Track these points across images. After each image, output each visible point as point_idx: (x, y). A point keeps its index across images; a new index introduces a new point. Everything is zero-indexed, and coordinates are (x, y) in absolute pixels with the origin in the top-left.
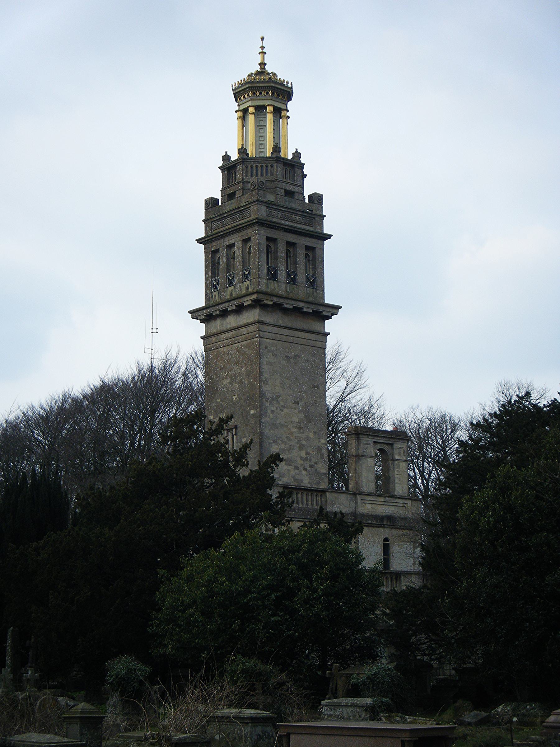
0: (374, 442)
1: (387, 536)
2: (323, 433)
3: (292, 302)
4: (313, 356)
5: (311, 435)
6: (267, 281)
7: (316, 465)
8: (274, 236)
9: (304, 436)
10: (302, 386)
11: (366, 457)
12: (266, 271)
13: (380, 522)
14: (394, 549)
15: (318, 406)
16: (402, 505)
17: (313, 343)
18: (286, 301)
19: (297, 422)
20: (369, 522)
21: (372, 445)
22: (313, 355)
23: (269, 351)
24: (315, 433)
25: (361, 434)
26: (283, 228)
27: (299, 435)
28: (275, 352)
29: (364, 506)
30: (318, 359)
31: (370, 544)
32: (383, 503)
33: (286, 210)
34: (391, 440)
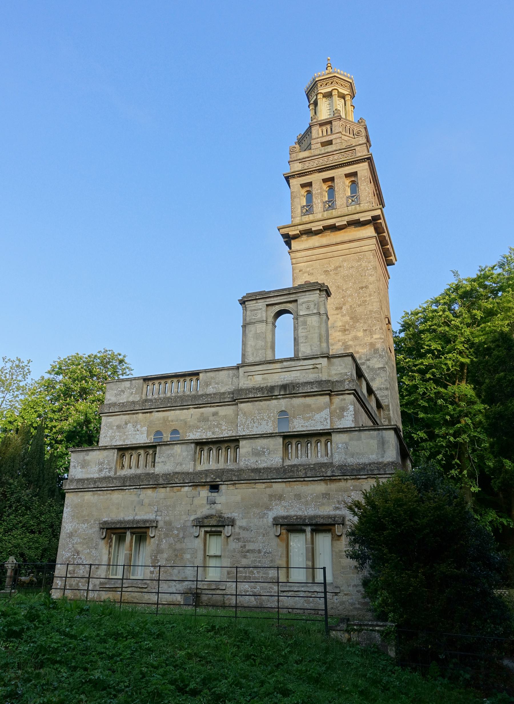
0: (268, 305)
1: (283, 409)
2: (375, 328)
3: (321, 223)
4: (358, 261)
5: (360, 334)
7: (368, 362)
9: (350, 337)
10: (345, 292)
11: (254, 323)
12: (299, 210)
13: (268, 393)
14: (295, 423)
15: (368, 304)
16: (311, 367)
17: (358, 250)
19: (340, 326)
20: (250, 396)
21: (264, 308)
22: (359, 260)
23: (305, 273)
24: (365, 331)
25: (247, 301)
27: (343, 338)
28: (311, 272)
29: (251, 379)
30: (366, 262)
31: (254, 422)
32: (280, 370)
34: (291, 296)
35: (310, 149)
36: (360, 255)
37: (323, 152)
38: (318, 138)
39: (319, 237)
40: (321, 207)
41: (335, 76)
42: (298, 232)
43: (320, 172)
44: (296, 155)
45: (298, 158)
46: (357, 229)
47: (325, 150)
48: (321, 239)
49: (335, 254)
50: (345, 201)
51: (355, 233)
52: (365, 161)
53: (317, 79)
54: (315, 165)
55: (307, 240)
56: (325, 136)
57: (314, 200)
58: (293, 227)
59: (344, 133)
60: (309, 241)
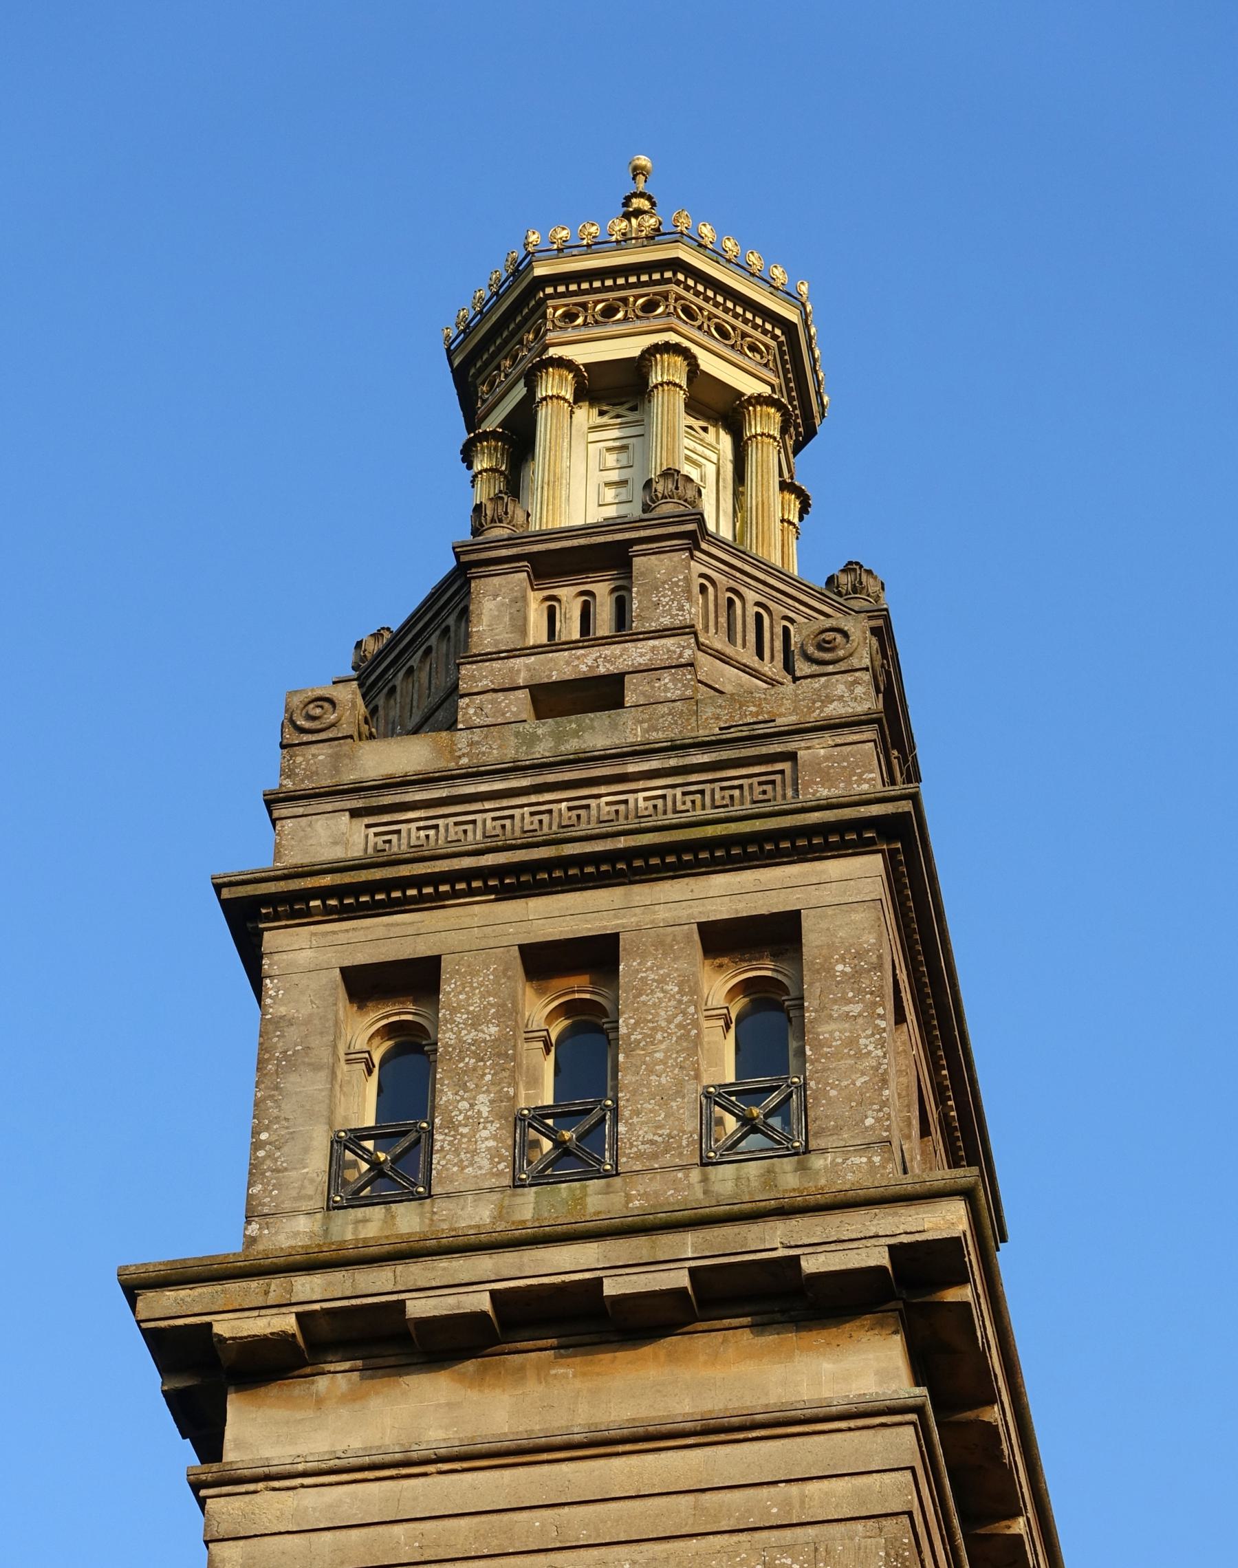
3: (484, 1265)
6: (327, 1219)
8: (422, 949)
12: (317, 1162)
17: (770, 1504)
18: (416, 1273)
26: (467, 875)
33: (525, 782)
35: (451, 726)
36: (785, 1549)
37: (543, 750)
38: (513, 653)
39: (462, 1378)
40: (494, 1154)
41: (677, 265)
42: (287, 1323)
43: (506, 893)
44: (336, 757)
45: (349, 777)
46: (770, 1339)
47: (559, 738)
48: (473, 1395)
49: (579, 1523)
50: (692, 1125)
51: (748, 1368)
52: (861, 847)
53: (539, 271)
54: (475, 837)
55: (352, 1397)
56: (572, 645)
57: (446, 1095)
58: (254, 1284)
59: (718, 642)
60: (375, 1403)
